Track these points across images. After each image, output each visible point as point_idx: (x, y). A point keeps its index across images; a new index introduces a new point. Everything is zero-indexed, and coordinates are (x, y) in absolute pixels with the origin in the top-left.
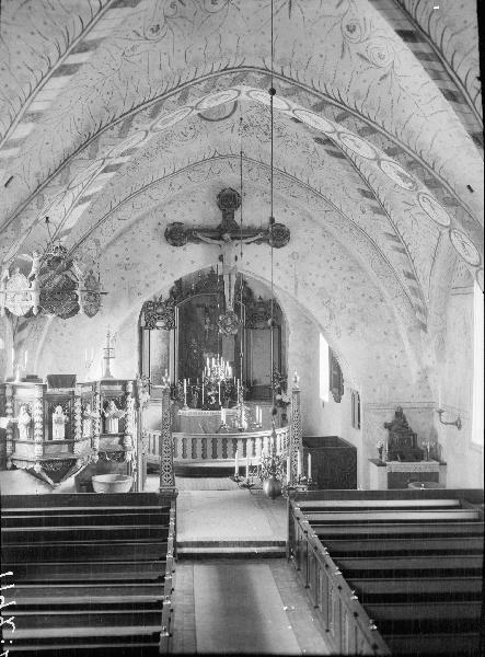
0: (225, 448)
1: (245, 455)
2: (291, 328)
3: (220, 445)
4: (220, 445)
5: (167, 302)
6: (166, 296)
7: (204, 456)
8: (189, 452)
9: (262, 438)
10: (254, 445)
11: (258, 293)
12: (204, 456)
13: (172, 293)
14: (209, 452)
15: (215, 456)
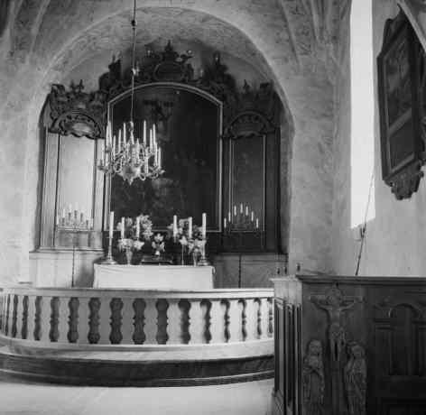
0: (139, 320)
1: (186, 338)
2: (296, 125)
3: (128, 314)
4: (128, 314)
5: (92, 96)
6: (92, 85)
7: (93, 338)
8: (63, 328)
9: (242, 301)
10: (207, 317)
11: (243, 77)
12: (93, 338)
13: (103, 79)
14: (105, 329)
15: (115, 338)
